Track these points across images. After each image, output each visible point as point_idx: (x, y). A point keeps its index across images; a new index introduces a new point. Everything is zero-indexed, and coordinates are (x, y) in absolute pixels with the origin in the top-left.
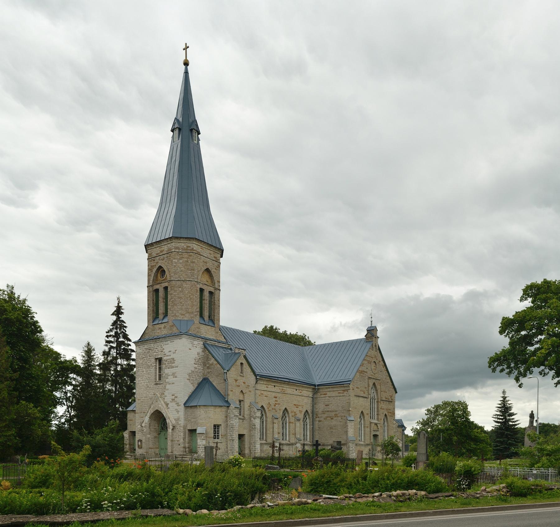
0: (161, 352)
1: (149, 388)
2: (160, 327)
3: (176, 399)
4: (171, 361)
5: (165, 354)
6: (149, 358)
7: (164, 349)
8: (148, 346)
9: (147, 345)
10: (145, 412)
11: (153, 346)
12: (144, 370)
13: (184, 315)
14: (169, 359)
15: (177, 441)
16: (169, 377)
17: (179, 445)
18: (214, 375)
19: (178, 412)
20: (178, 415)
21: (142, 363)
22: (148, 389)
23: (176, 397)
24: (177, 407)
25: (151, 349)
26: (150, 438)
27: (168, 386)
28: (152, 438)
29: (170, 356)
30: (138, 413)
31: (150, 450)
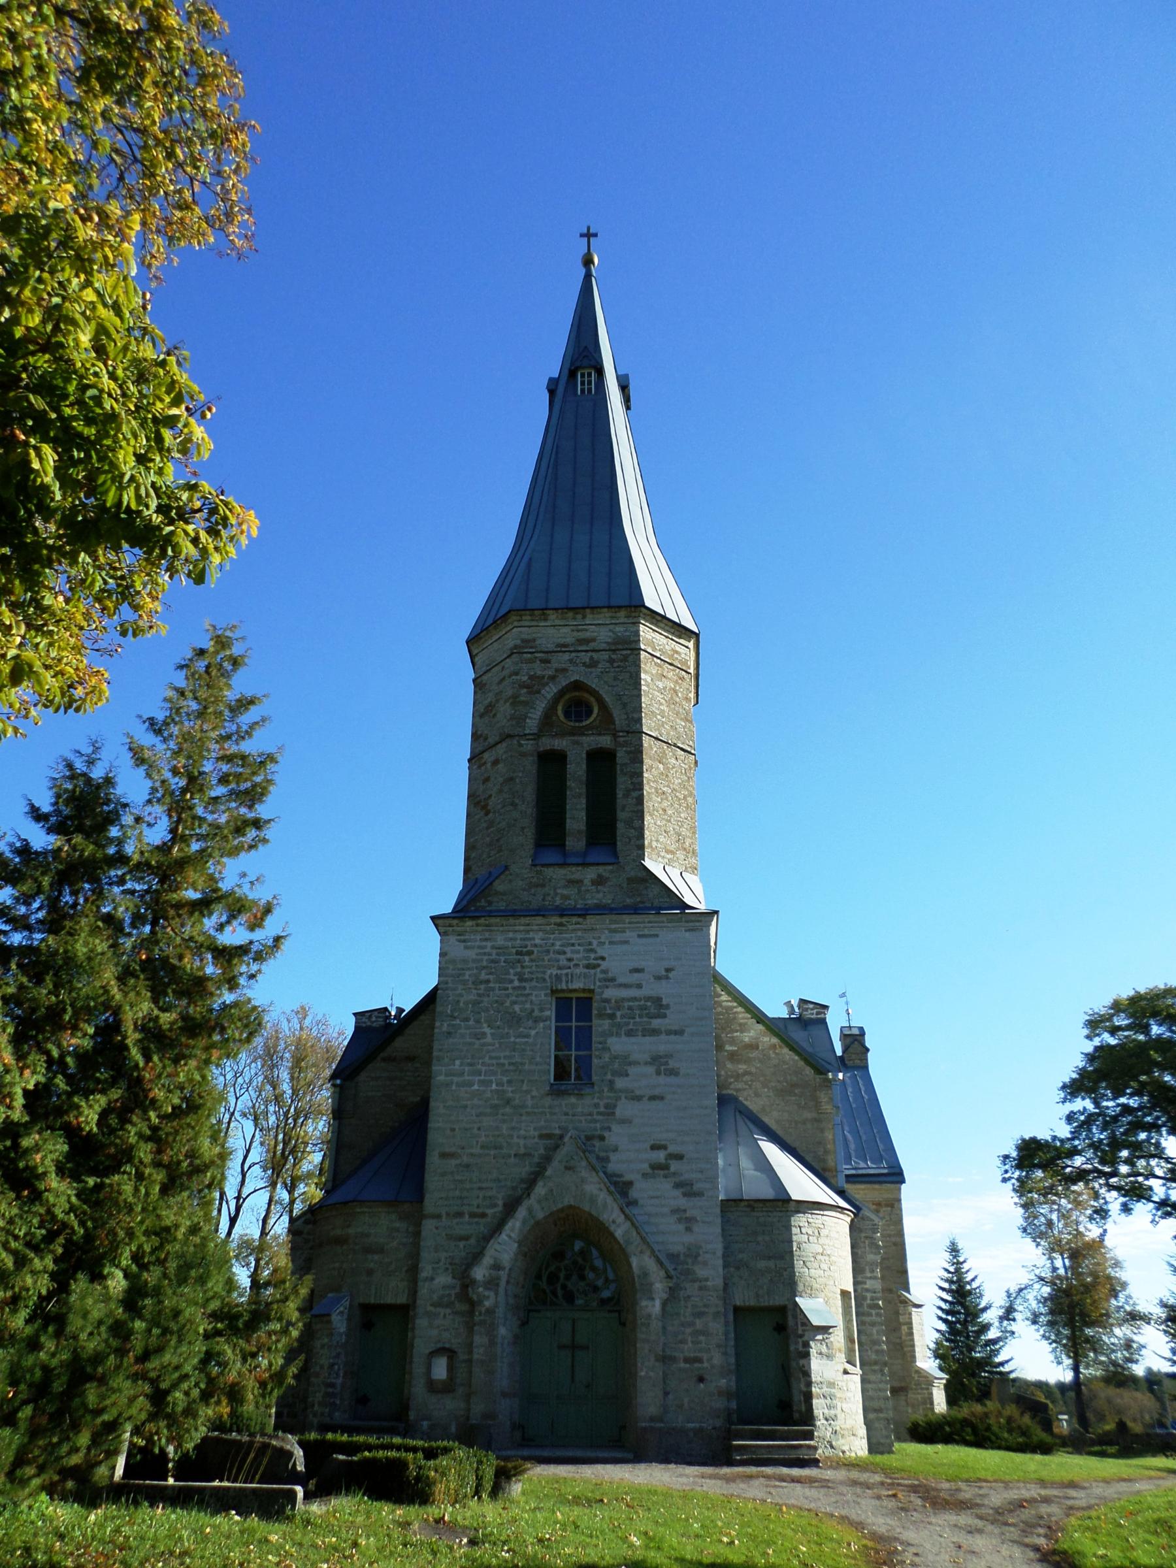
0: (588, 967)
2: (576, 876)
3: (674, 1166)
4: (645, 1008)
5: (613, 980)
6: (516, 983)
7: (603, 958)
8: (511, 939)
9: (511, 935)
10: (484, 1215)
11: (537, 941)
12: (488, 1030)
13: (672, 852)
14: (634, 999)
15: (686, 1360)
16: (632, 1070)
17: (701, 1379)
18: (765, 1086)
19: (688, 1222)
20: (688, 1239)
21: (476, 1003)
22: (508, 1110)
23: (679, 1157)
24: (683, 1202)
25: (530, 953)
27: (624, 1109)
29: (639, 986)
30: (438, 1217)
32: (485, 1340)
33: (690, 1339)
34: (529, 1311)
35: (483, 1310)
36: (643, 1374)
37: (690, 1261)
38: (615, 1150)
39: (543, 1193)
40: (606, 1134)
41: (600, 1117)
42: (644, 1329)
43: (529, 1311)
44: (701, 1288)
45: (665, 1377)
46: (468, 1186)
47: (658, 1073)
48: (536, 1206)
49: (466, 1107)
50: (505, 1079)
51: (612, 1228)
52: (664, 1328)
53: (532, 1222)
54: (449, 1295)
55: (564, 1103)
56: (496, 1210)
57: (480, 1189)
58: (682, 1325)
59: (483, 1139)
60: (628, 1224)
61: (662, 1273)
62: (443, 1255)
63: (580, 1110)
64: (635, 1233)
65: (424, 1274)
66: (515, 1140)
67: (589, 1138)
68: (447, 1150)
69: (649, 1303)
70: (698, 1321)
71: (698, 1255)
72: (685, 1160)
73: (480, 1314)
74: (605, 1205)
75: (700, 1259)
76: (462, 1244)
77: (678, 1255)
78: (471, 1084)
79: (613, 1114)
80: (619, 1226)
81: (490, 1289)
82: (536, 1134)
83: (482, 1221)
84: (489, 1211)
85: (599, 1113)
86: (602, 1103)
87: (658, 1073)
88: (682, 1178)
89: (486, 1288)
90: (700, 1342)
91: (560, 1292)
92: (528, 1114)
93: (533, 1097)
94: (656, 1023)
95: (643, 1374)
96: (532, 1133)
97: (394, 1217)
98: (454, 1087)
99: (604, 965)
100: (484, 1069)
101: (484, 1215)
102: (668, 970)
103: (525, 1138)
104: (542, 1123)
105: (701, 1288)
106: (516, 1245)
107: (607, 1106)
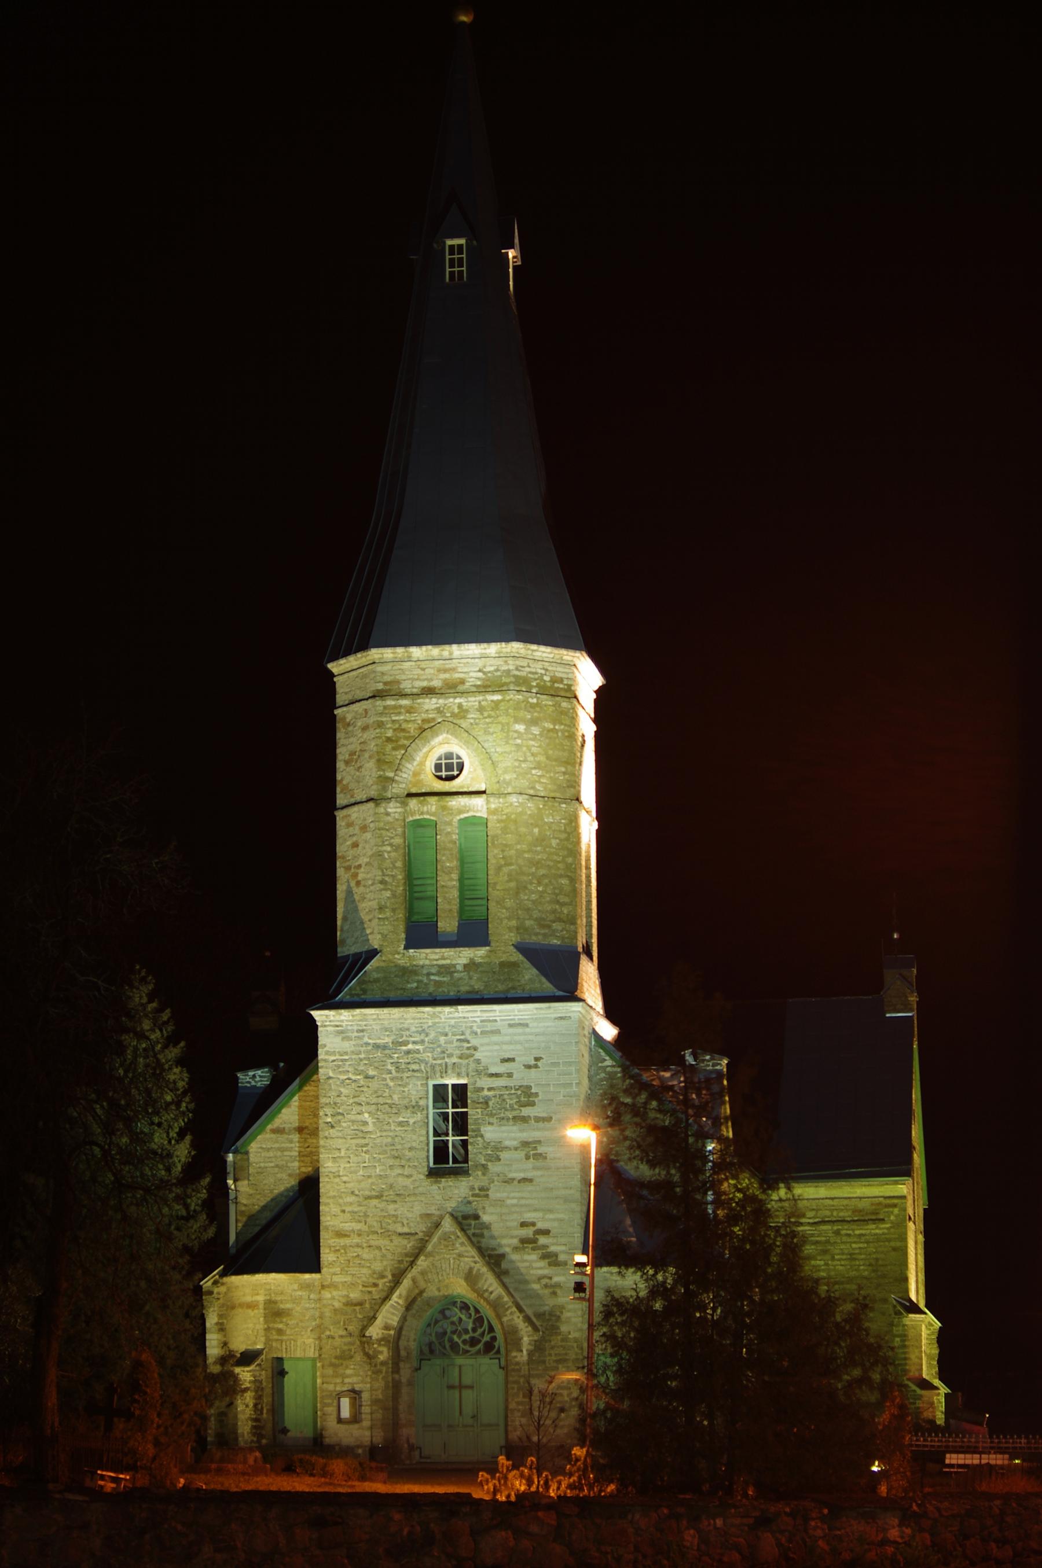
3: (542, 1240)
16: (503, 1155)
23: (546, 1232)
43: (421, 1360)
47: (527, 1157)
56: (385, 1280)
69: (518, 1354)
79: (487, 1196)
87: (527, 1157)
94: (526, 1111)
99: (478, 1055)
102: (537, 1059)
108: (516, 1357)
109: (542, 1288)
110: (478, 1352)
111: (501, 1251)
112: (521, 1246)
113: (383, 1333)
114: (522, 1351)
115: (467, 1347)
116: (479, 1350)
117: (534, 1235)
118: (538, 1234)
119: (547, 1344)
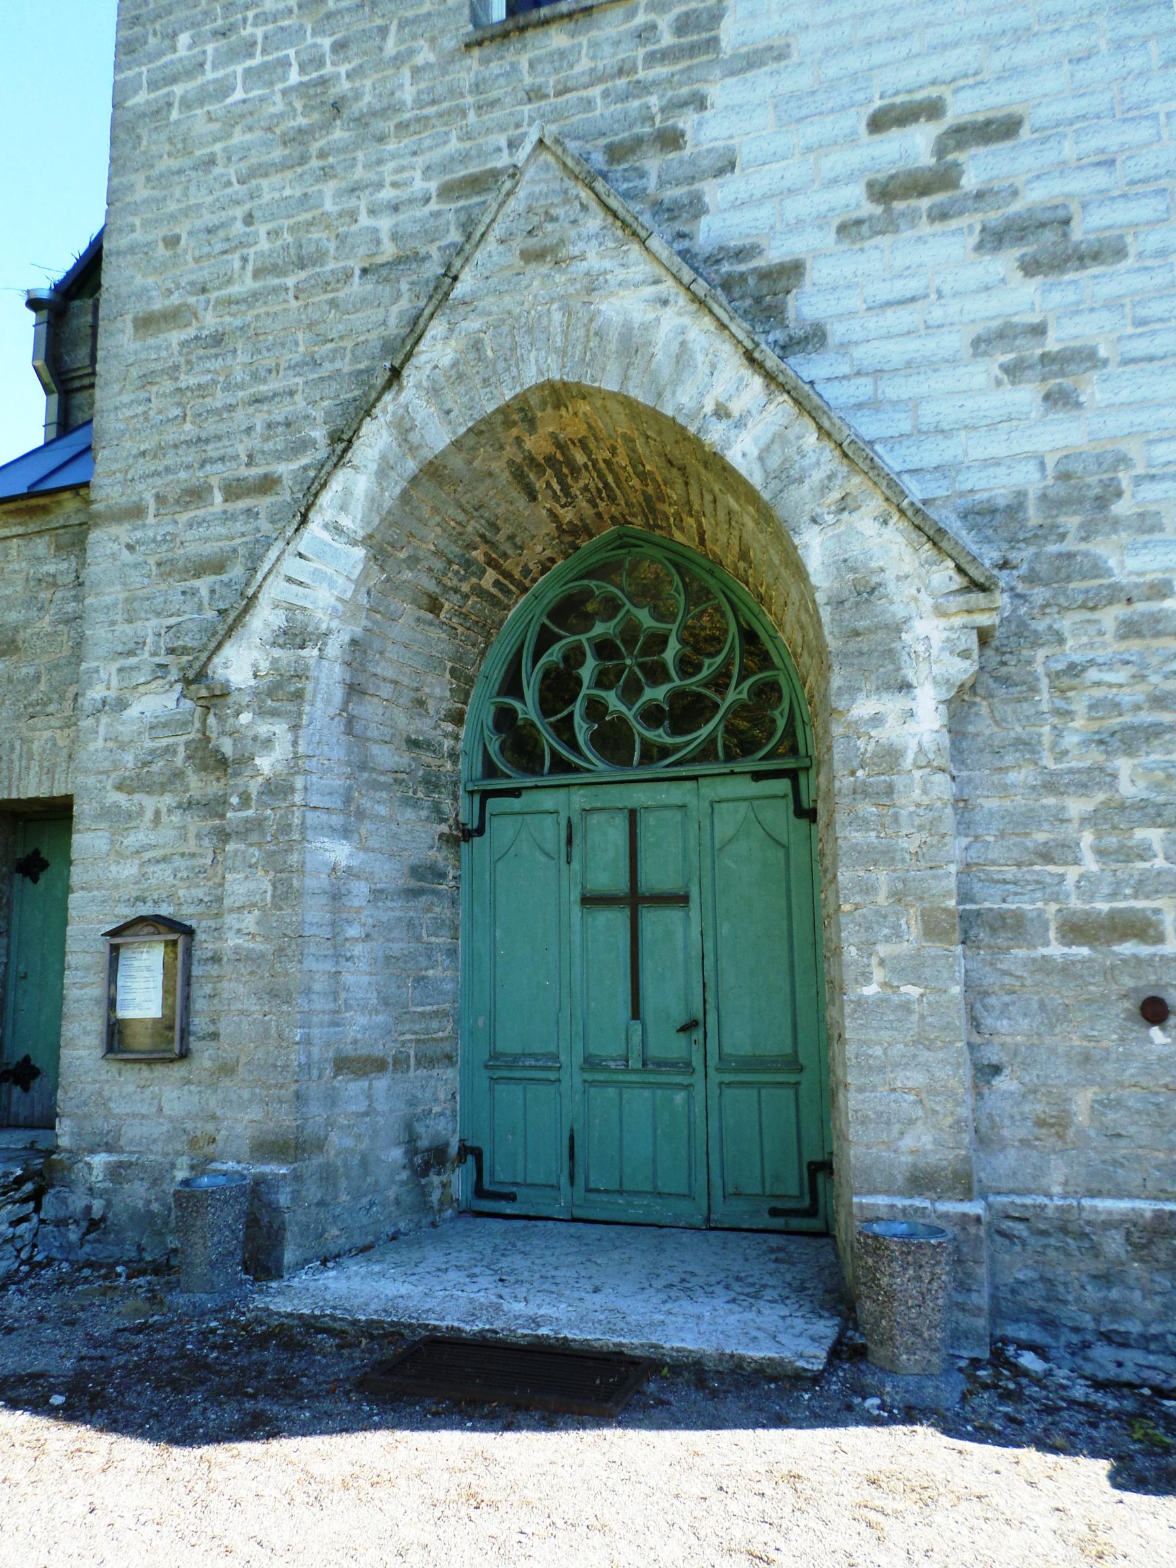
1: (360, 121)
10: (267, 484)
22: (338, 134)
26: (360, 889)
28: (377, 894)
30: (136, 512)
31: (353, 1089)
32: (264, 883)
33: (1087, 838)
34: (486, 795)
35: (254, 786)
36: (870, 990)
37: (1071, 522)
38: (727, 166)
39: (446, 361)
40: (687, 121)
41: (661, 71)
42: (867, 809)
43: (486, 795)
44: (1130, 629)
45: (975, 992)
46: (220, 399)
48: (423, 411)
49: (211, 161)
50: (326, 43)
51: (715, 434)
52: (962, 804)
53: (411, 466)
54: (170, 750)
55: (524, 62)
57: (257, 400)
58: (1051, 786)
59: (264, 245)
60: (782, 409)
61: (944, 576)
62: (149, 626)
63: (584, 64)
64: (811, 439)
65: (96, 693)
66: (364, 220)
67: (616, 153)
68: (158, 305)
69: (890, 705)
70: (1123, 765)
71: (1111, 492)
72: (1025, 133)
73: (245, 800)
74: (682, 357)
75: (1121, 508)
76: (203, 585)
77: (1015, 509)
78: (223, 89)
80: (740, 424)
81: (274, 713)
82: (433, 186)
83: (263, 503)
84: (284, 469)
85: (652, 59)
86: (665, 22)
88: (1016, 207)
89: (262, 713)
90: (1144, 853)
91: (582, 730)
92: (402, 126)
93: (416, 71)
95: (870, 990)
96: (419, 185)
97: (41, 546)
98: (175, 115)
100: (259, 32)
101: (267, 484)
103: (396, 209)
104: (454, 145)
105: (1130, 629)
106: (360, 553)
107: (682, 26)
108: (877, 720)
109: (999, 383)
110: (706, 753)
111: (775, 254)
112: (878, 210)
113: (275, 661)
114: (905, 687)
115: (660, 736)
116: (711, 740)
117: (941, 150)
118: (960, 146)
119: (1041, 654)
